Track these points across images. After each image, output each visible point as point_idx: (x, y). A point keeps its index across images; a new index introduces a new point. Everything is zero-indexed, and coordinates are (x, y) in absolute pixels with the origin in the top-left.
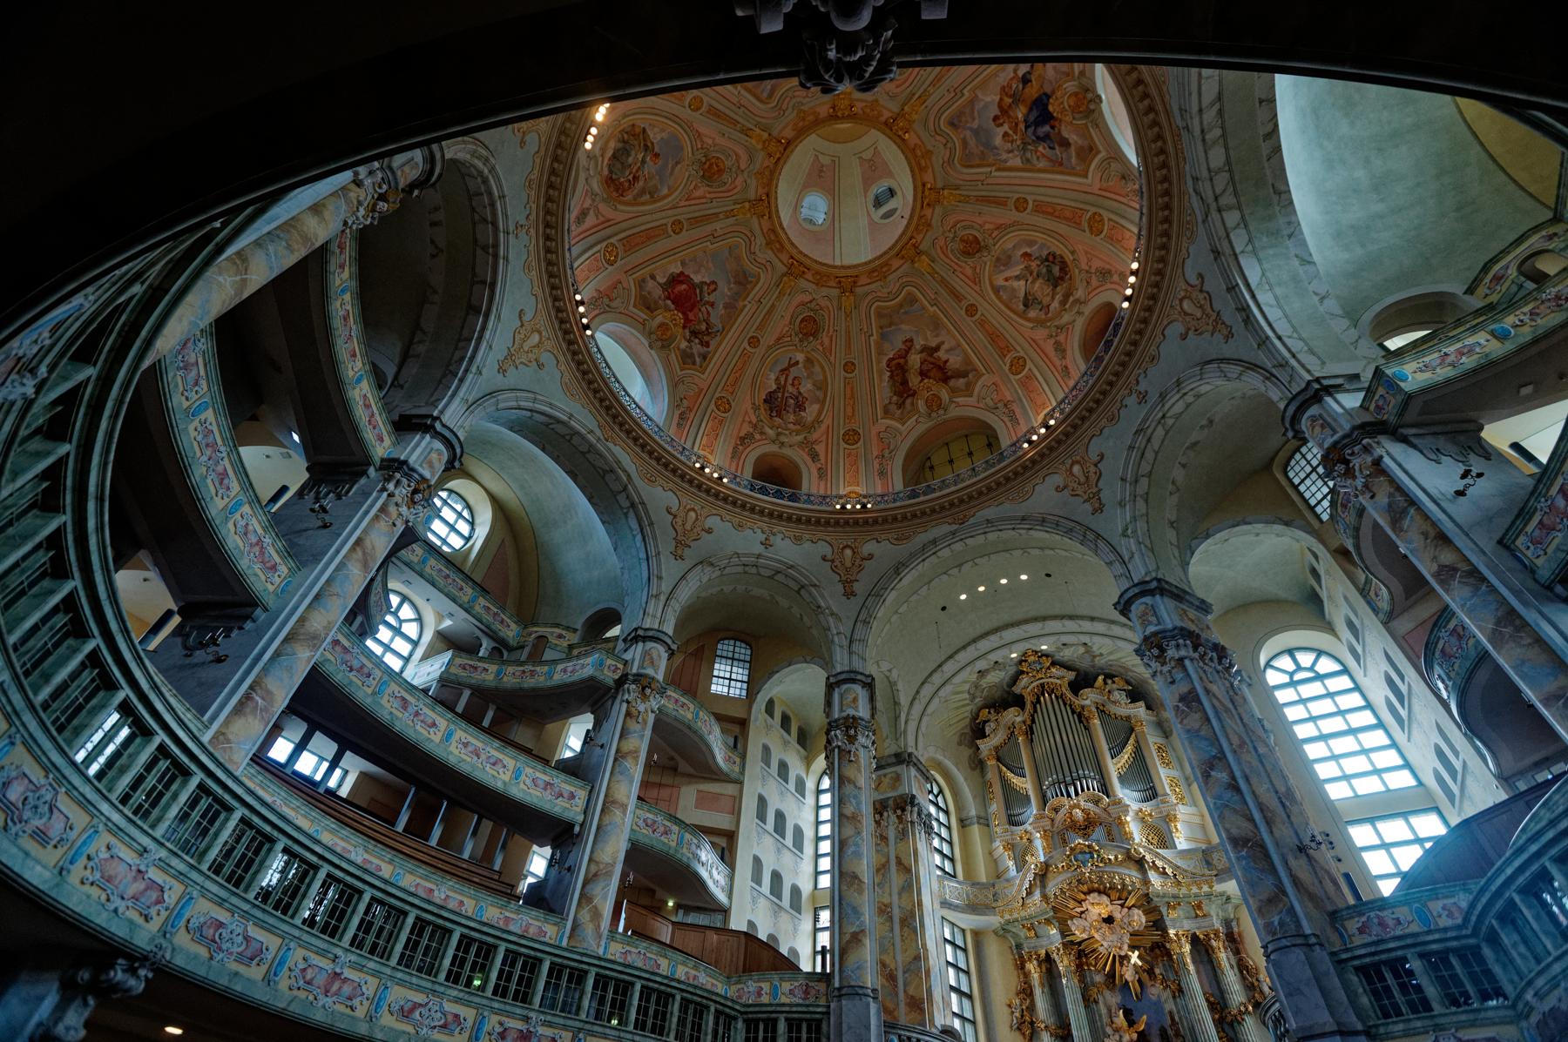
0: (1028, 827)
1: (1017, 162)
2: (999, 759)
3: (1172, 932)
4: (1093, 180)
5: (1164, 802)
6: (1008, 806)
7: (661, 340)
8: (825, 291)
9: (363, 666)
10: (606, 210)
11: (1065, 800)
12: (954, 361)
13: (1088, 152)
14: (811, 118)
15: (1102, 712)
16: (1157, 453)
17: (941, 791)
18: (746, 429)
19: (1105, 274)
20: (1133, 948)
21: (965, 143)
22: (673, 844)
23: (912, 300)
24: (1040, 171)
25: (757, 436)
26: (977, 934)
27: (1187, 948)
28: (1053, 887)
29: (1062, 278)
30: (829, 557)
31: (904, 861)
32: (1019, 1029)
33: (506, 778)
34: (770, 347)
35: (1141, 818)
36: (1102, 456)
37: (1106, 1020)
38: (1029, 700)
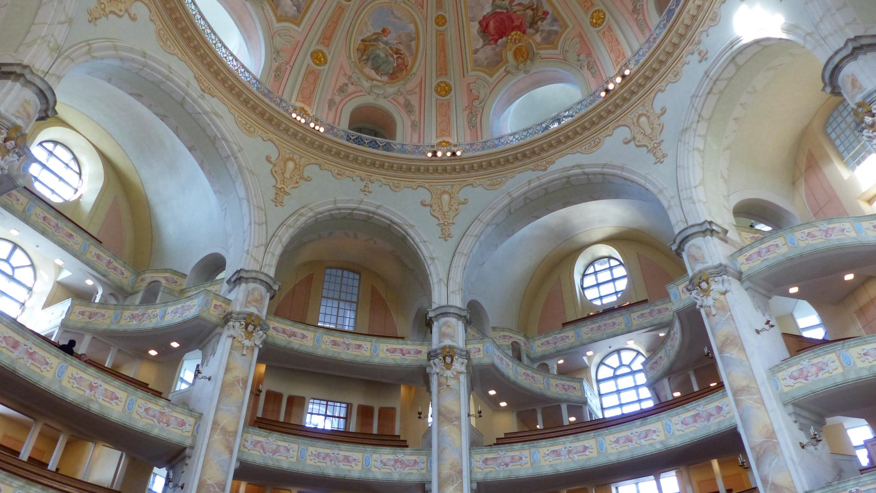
9: (513, 457)
10: (413, 83)
22: (840, 370)
33: (662, 437)
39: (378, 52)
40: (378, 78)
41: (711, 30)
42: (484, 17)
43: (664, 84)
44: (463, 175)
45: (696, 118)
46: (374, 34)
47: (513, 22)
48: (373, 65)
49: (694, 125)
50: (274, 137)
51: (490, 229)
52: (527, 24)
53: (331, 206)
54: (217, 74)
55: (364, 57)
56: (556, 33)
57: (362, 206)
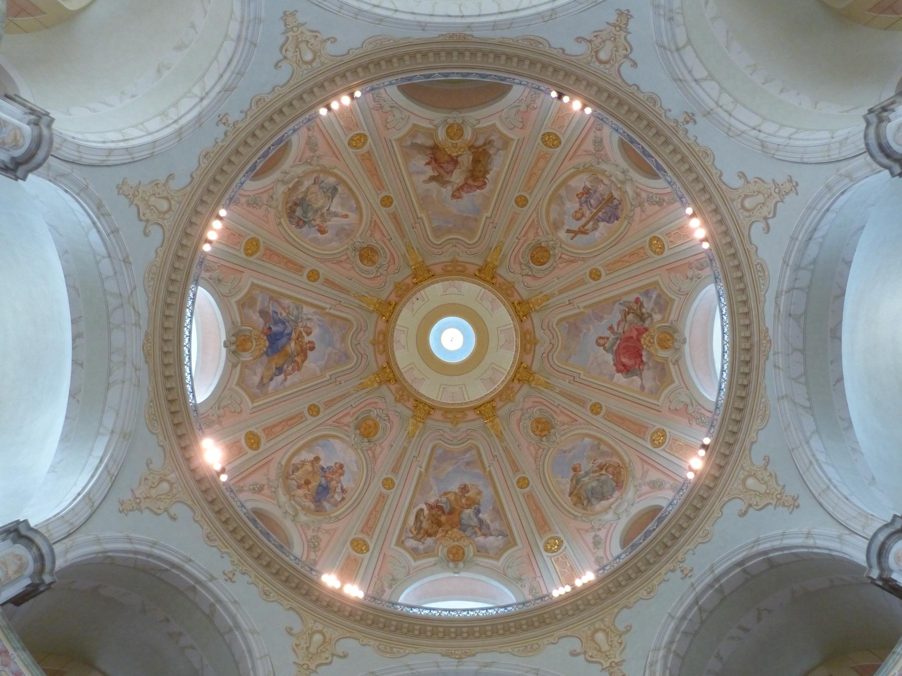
1: (306, 309)
4: (247, 281)
7: (671, 338)
8: (510, 277)
12: (420, 162)
13: (246, 303)
14: (450, 416)
16: (216, 58)
18: (651, 209)
19: (254, 203)
21: (343, 339)
23: (438, 231)
24: (289, 297)
25: (644, 195)
29: (296, 204)
30: (627, 64)
34: (584, 260)
36: (277, 66)
39: (589, 487)
40: (611, 500)
41: (666, 106)
42: (615, 365)
43: (714, 171)
44: (737, 448)
45: (754, 133)
46: (572, 480)
47: (632, 337)
48: (597, 498)
49: (762, 136)
50: (563, 632)
51: (816, 443)
52: (640, 323)
53: (672, 625)
54: (458, 634)
55: (585, 503)
56: (659, 296)
57: (699, 588)
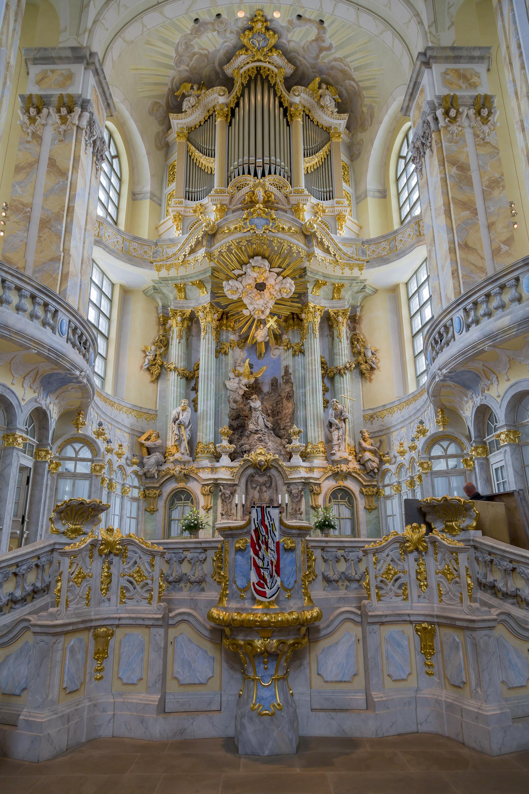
0: (205, 201)
2: (188, 140)
3: (311, 305)
5: (338, 203)
6: (188, 182)
11: (250, 180)
15: (307, 116)
17: (117, 156)
20: (272, 314)
26: (126, 292)
27: (318, 320)
28: (220, 245)
31: (59, 163)
32: (148, 369)
35: (316, 214)
37: (230, 367)
38: (238, 82)
